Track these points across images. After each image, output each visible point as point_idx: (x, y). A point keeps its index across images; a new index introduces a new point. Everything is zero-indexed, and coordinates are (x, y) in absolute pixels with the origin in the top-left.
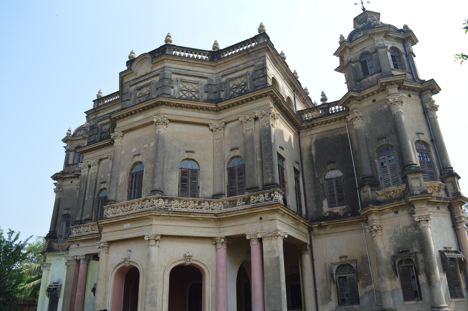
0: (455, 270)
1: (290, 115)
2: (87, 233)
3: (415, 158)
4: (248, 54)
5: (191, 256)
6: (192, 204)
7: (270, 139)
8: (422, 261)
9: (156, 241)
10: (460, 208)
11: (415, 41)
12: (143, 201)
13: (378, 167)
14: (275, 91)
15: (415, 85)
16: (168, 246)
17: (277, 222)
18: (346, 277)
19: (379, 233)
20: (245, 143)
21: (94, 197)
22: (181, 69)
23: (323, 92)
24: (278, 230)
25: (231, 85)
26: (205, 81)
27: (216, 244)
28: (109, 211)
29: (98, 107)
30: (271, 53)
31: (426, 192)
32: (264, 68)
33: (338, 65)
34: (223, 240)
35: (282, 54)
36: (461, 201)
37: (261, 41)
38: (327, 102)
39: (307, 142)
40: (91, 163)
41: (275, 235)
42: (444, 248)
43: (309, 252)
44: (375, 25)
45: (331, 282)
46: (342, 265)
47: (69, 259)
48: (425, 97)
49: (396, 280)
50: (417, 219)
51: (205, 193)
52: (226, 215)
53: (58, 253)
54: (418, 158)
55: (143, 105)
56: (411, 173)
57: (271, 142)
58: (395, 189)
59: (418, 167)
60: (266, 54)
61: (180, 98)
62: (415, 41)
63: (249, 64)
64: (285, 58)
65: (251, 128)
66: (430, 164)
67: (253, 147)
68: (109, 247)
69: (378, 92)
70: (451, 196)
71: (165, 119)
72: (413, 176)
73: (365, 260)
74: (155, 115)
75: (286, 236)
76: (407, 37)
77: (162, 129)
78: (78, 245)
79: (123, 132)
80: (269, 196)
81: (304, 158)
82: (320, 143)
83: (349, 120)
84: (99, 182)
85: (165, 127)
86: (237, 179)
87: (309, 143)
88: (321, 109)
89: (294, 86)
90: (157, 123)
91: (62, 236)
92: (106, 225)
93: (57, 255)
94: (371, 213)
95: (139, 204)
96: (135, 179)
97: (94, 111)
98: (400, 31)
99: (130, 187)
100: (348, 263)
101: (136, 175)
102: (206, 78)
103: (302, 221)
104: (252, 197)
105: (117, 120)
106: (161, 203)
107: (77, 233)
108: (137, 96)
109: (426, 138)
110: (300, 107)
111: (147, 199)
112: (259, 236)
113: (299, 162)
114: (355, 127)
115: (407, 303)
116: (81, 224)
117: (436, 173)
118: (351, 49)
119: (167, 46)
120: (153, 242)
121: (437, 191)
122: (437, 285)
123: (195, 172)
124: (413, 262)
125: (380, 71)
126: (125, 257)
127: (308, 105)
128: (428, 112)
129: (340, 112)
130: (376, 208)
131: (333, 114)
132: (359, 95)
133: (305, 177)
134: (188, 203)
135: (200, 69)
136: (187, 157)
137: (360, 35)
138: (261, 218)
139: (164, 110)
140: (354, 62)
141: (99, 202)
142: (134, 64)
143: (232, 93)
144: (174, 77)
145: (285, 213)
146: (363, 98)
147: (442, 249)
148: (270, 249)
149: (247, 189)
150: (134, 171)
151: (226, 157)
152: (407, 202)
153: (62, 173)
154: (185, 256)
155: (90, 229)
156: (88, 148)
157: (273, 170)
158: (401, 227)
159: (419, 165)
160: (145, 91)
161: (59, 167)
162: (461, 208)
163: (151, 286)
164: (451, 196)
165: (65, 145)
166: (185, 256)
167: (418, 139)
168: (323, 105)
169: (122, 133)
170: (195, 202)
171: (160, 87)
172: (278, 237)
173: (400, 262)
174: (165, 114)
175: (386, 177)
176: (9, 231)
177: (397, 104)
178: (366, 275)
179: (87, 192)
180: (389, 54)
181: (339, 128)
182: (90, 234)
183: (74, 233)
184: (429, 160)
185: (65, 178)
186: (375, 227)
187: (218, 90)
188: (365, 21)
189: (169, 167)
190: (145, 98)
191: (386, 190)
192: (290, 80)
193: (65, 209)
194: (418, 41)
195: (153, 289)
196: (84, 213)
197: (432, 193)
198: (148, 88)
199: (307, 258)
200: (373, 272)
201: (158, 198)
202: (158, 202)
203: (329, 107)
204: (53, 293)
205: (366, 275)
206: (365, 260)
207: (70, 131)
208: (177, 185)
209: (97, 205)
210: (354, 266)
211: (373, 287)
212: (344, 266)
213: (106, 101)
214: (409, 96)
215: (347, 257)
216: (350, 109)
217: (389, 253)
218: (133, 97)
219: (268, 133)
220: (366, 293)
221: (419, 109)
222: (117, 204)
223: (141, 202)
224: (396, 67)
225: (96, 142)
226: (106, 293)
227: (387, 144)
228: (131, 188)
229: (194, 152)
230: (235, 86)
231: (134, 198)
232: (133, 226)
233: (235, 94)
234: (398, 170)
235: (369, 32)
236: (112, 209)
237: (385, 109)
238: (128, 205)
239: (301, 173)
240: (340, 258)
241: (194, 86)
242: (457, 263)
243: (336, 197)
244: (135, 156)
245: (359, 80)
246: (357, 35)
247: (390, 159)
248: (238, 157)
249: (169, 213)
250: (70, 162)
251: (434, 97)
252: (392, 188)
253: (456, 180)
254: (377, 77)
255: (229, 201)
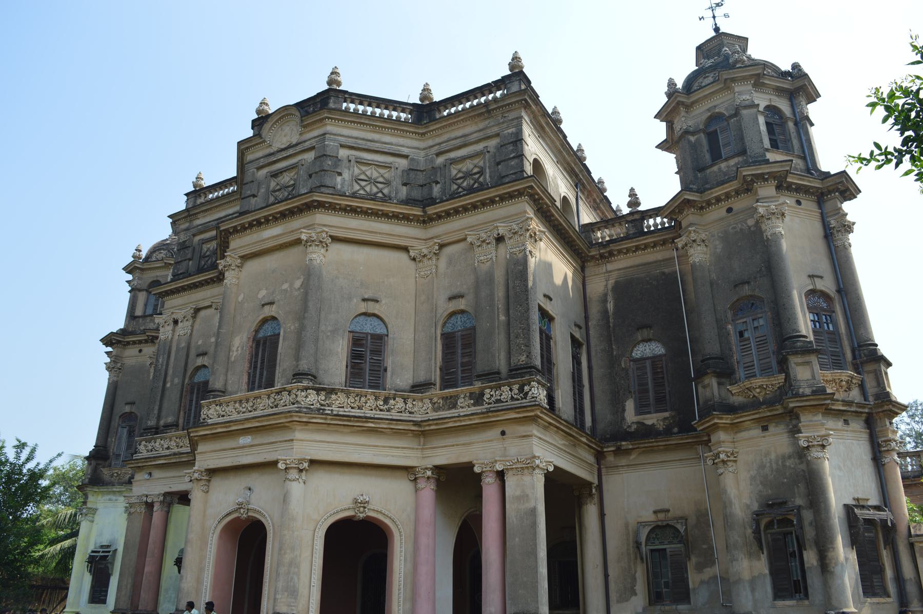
0: (874, 543)
1: (568, 232)
2: (167, 452)
3: (804, 324)
4: (489, 112)
5: (367, 502)
6: (371, 402)
7: (526, 280)
8: (811, 524)
9: (301, 471)
10: (888, 423)
11: (812, 95)
12: (278, 393)
13: (734, 339)
14: (538, 187)
15: (809, 181)
16: (323, 481)
17: (535, 441)
18: (665, 550)
19: (731, 467)
20: (477, 287)
21: (183, 382)
22: (356, 138)
23: (632, 190)
24: (534, 457)
25: (454, 172)
26: (403, 163)
27: (416, 479)
28: (211, 411)
29: (194, 207)
30: (533, 112)
31: (820, 391)
32: (518, 140)
33: (663, 137)
34: (429, 473)
35: (555, 112)
36: (891, 411)
37: (515, 88)
38: (641, 208)
39: (598, 285)
40: (179, 315)
41: (529, 466)
42: (854, 499)
43: (596, 499)
44: (736, 62)
45: (636, 558)
46: (657, 527)
47: (133, 500)
48: (828, 206)
49: (759, 559)
50: (803, 443)
51: (398, 381)
52: (437, 424)
53: (110, 489)
54: (810, 324)
55: (282, 207)
56: (796, 353)
57: (527, 286)
58: (763, 384)
59: (810, 342)
60: (523, 114)
61: (354, 195)
62: (812, 95)
63: (490, 132)
64: (560, 121)
65: (490, 256)
66: (834, 337)
67: (492, 295)
68: (209, 481)
69: (737, 193)
70: (871, 399)
71: (324, 235)
72: (799, 359)
73: (702, 518)
74: (304, 228)
75: (551, 469)
76: (798, 86)
77: (317, 256)
78: (150, 474)
79: (242, 257)
80: (521, 390)
81: (591, 317)
82: (623, 289)
83: (680, 246)
84: (193, 353)
85: (323, 251)
86: (460, 356)
87: (602, 288)
88: (627, 222)
89: (577, 175)
90: (309, 242)
91: (120, 455)
92: (204, 438)
93: (109, 493)
94: (716, 427)
95: (269, 398)
96: (264, 350)
97: (186, 214)
98: (785, 74)
99: (253, 365)
100: (670, 523)
101: (265, 343)
102: (406, 157)
103: (584, 440)
104: (488, 391)
105: (231, 234)
106: (313, 398)
107: (148, 451)
108: (271, 188)
109: (827, 285)
110: (587, 217)
111: (284, 390)
112: (499, 467)
113: (582, 324)
114: (691, 260)
115: (780, 603)
116: (157, 433)
117: (844, 355)
118: (688, 107)
119: (332, 93)
120: (293, 474)
121: (844, 388)
122: (838, 570)
123: (379, 340)
124: (793, 526)
125: (743, 152)
126: (240, 500)
127: (603, 213)
128: (834, 236)
129: (664, 228)
130: (726, 420)
131: (650, 232)
132: (701, 197)
133: (593, 353)
134: (363, 399)
135: (394, 140)
136: (364, 311)
137: (707, 81)
138: (503, 433)
139: (322, 218)
140: (693, 134)
141: (192, 393)
142: (267, 126)
143: (455, 187)
144: (343, 153)
145: (550, 424)
146: (709, 203)
147: (850, 502)
148: (518, 493)
149: (478, 376)
150: (261, 335)
151: (440, 311)
152: (785, 408)
153: (123, 332)
154: (356, 501)
155: (173, 443)
156: (174, 286)
157: (529, 340)
158: (773, 456)
159: (811, 338)
160: (286, 179)
161: (118, 322)
162: (891, 423)
163: (287, 558)
164: (871, 399)
165: (130, 277)
166: (356, 501)
167: (811, 287)
168: (631, 214)
169: (239, 261)
170: (376, 399)
171: (316, 173)
172: (534, 469)
173: (769, 525)
174: (324, 225)
175: (748, 360)
176: (17, 443)
177: (773, 218)
178: (705, 546)
179: (170, 372)
180: (761, 120)
181: (660, 261)
182: (175, 454)
183: (144, 450)
184: (831, 328)
185: (128, 343)
186: (722, 456)
187: (428, 181)
188: (718, 53)
189: (330, 328)
190: (286, 194)
191: (747, 384)
192: (568, 164)
193: (127, 404)
194: (819, 96)
195: (294, 564)
196: (164, 413)
197: (834, 394)
198: (292, 174)
199: (591, 512)
200: (718, 543)
201: (306, 389)
202: (306, 397)
203: (643, 219)
204: (100, 564)
205: (705, 546)
206: (702, 518)
207: (140, 251)
208: (344, 363)
209: (188, 398)
210: (682, 529)
211: (716, 570)
212: (663, 529)
213: (211, 196)
214: (799, 203)
215: (668, 511)
216: (684, 224)
217: (748, 506)
218: (262, 190)
219: (521, 268)
220: (702, 582)
221: (816, 228)
222: (227, 398)
223: (273, 395)
224: (775, 145)
225: (190, 275)
226: (201, 570)
227: (751, 296)
228: (255, 367)
229: (377, 301)
230: (460, 175)
231: (260, 387)
232: (256, 442)
233: (460, 190)
234: (772, 346)
235: (725, 75)
236: (218, 408)
237: (750, 227)
238: (247, 401)
239: (584, 347)
240: (655, 512)
241: (382, 171)
242: (879, 529)
243: (651, 394)
244: (263, 305)
245: (702, 170)
246: (701, 80)
247: (756, 324)
248: (462, 312)
249: (326, 419)
250: (139, 312)
251: (847, 206)
252: (758, 382)
253: (883, 368)
254: (736, 164)
255: (443, 398)
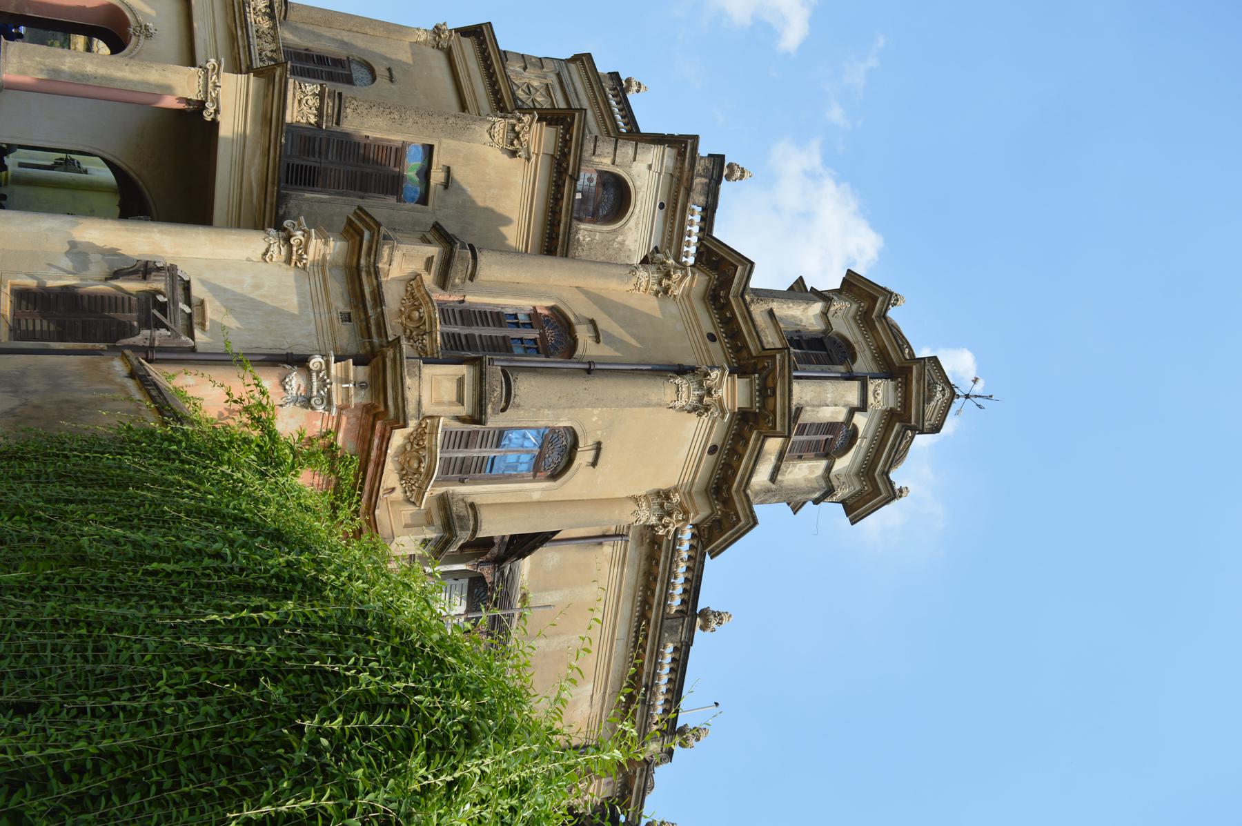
167: (572, 319)
229: (391, 79)
